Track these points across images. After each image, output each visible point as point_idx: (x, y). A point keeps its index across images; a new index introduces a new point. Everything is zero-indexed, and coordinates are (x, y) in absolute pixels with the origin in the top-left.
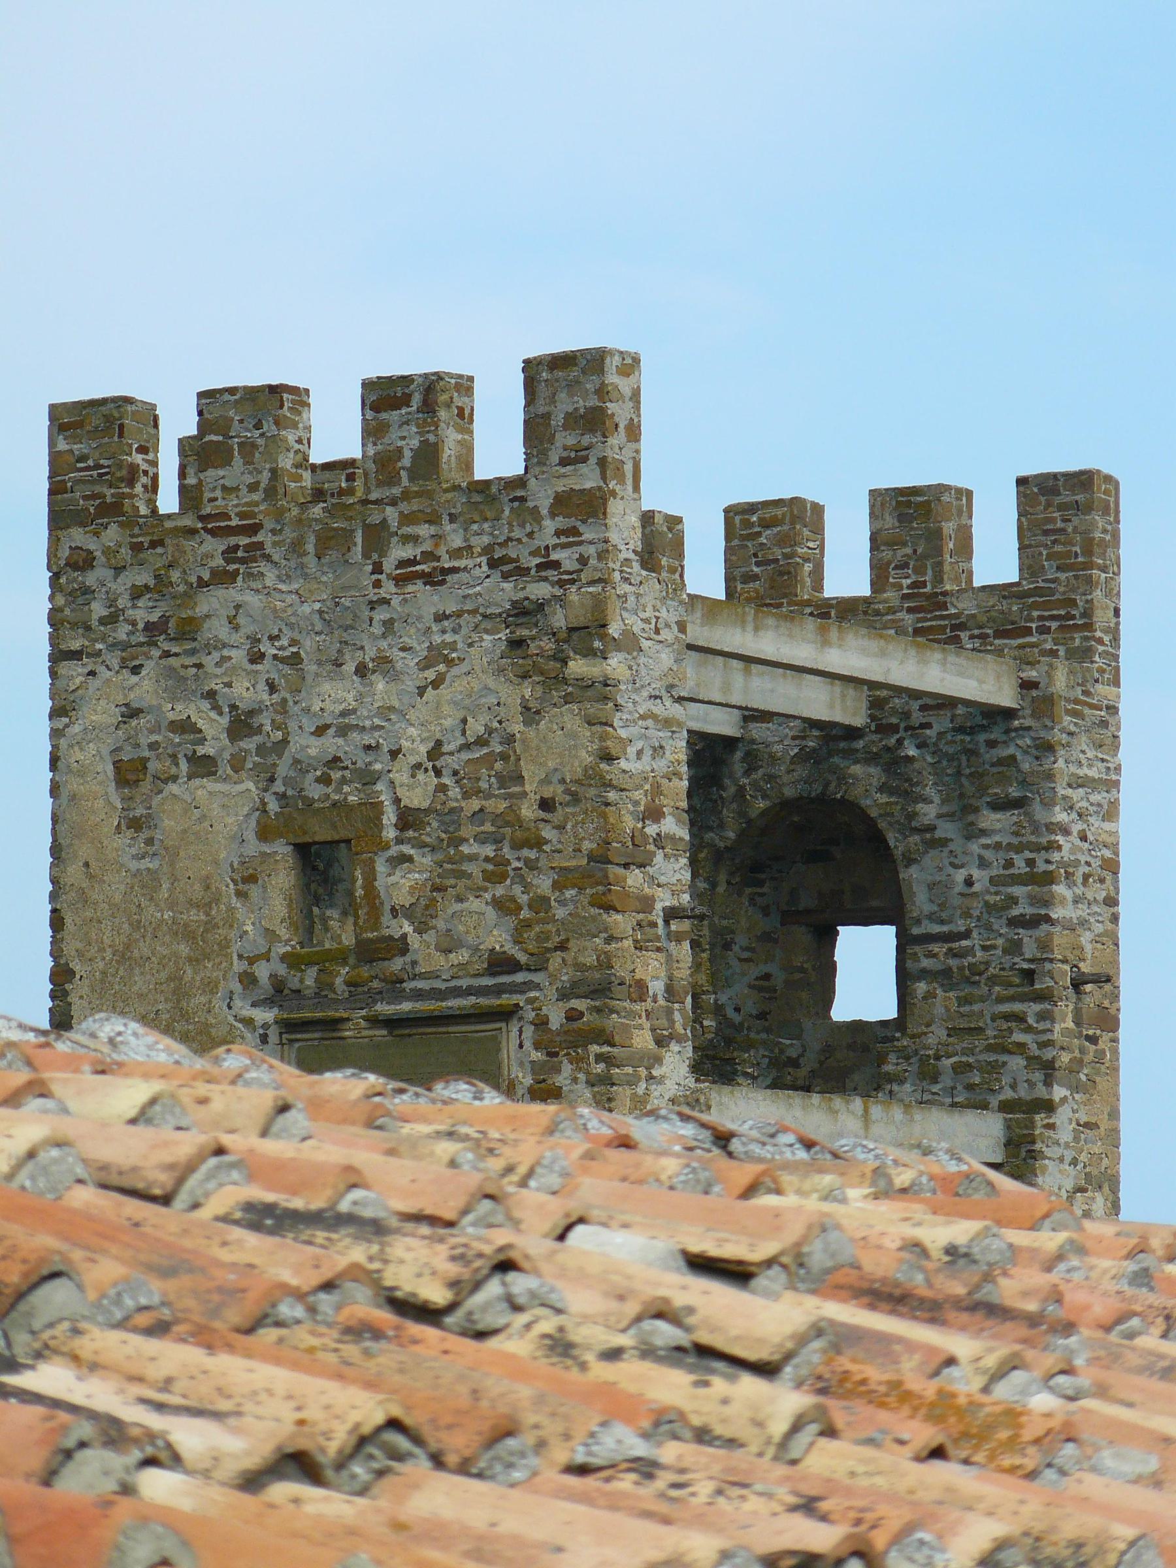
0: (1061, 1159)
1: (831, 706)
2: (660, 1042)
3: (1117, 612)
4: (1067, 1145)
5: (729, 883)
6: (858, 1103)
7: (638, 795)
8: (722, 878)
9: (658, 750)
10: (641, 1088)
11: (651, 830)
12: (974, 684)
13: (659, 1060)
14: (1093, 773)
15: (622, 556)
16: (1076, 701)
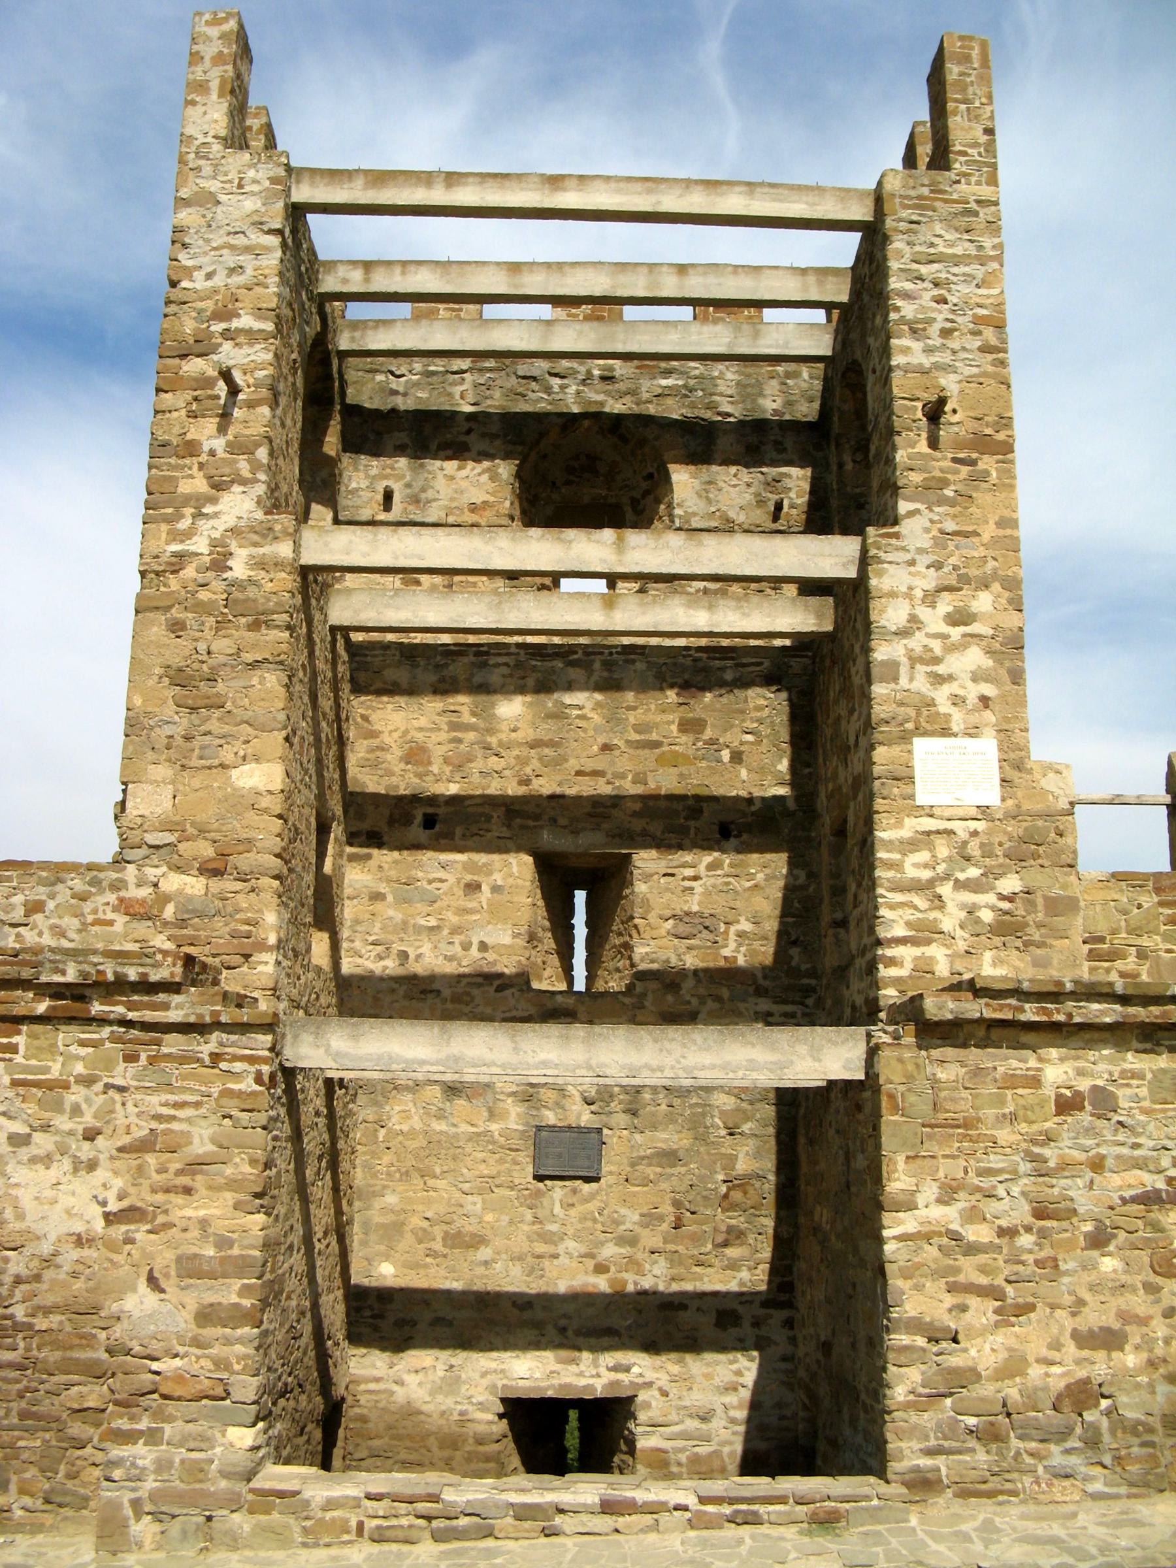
0: (912, 563)
1: (805, 288)
2: (219, 486)
3: (990, 131)
4: (920, 551)
5: (854, 461)
6: (608, 534)
7: (200, 305)
8: (847, 458)
9: (238, 269)
10: (185, 524)
11: (217, 327)
12: (803, 206)
13: (214, 501)
14: (958, 250)
15: (202, 139)
16: (920, 197)
